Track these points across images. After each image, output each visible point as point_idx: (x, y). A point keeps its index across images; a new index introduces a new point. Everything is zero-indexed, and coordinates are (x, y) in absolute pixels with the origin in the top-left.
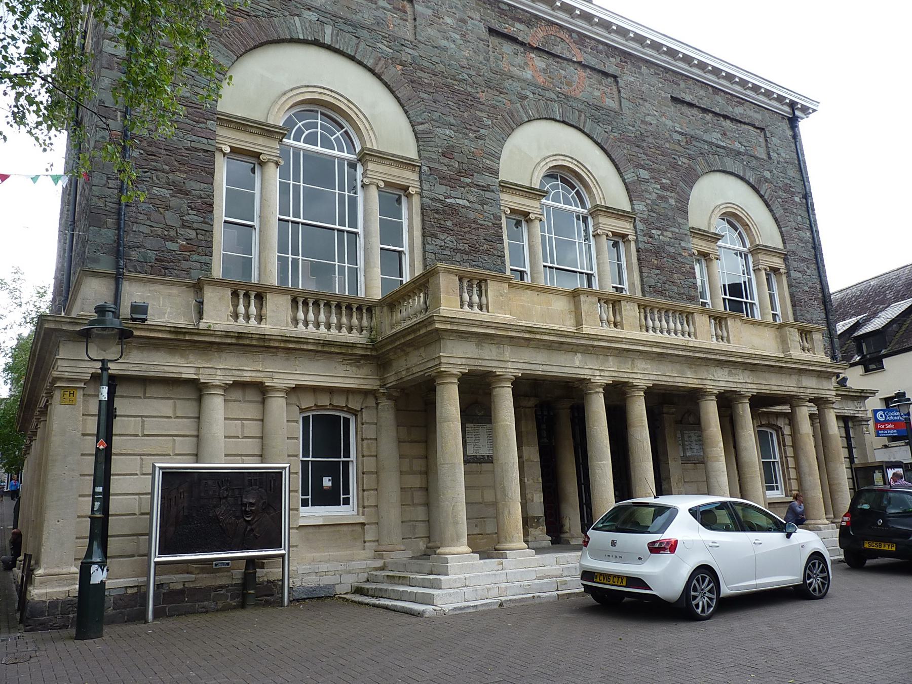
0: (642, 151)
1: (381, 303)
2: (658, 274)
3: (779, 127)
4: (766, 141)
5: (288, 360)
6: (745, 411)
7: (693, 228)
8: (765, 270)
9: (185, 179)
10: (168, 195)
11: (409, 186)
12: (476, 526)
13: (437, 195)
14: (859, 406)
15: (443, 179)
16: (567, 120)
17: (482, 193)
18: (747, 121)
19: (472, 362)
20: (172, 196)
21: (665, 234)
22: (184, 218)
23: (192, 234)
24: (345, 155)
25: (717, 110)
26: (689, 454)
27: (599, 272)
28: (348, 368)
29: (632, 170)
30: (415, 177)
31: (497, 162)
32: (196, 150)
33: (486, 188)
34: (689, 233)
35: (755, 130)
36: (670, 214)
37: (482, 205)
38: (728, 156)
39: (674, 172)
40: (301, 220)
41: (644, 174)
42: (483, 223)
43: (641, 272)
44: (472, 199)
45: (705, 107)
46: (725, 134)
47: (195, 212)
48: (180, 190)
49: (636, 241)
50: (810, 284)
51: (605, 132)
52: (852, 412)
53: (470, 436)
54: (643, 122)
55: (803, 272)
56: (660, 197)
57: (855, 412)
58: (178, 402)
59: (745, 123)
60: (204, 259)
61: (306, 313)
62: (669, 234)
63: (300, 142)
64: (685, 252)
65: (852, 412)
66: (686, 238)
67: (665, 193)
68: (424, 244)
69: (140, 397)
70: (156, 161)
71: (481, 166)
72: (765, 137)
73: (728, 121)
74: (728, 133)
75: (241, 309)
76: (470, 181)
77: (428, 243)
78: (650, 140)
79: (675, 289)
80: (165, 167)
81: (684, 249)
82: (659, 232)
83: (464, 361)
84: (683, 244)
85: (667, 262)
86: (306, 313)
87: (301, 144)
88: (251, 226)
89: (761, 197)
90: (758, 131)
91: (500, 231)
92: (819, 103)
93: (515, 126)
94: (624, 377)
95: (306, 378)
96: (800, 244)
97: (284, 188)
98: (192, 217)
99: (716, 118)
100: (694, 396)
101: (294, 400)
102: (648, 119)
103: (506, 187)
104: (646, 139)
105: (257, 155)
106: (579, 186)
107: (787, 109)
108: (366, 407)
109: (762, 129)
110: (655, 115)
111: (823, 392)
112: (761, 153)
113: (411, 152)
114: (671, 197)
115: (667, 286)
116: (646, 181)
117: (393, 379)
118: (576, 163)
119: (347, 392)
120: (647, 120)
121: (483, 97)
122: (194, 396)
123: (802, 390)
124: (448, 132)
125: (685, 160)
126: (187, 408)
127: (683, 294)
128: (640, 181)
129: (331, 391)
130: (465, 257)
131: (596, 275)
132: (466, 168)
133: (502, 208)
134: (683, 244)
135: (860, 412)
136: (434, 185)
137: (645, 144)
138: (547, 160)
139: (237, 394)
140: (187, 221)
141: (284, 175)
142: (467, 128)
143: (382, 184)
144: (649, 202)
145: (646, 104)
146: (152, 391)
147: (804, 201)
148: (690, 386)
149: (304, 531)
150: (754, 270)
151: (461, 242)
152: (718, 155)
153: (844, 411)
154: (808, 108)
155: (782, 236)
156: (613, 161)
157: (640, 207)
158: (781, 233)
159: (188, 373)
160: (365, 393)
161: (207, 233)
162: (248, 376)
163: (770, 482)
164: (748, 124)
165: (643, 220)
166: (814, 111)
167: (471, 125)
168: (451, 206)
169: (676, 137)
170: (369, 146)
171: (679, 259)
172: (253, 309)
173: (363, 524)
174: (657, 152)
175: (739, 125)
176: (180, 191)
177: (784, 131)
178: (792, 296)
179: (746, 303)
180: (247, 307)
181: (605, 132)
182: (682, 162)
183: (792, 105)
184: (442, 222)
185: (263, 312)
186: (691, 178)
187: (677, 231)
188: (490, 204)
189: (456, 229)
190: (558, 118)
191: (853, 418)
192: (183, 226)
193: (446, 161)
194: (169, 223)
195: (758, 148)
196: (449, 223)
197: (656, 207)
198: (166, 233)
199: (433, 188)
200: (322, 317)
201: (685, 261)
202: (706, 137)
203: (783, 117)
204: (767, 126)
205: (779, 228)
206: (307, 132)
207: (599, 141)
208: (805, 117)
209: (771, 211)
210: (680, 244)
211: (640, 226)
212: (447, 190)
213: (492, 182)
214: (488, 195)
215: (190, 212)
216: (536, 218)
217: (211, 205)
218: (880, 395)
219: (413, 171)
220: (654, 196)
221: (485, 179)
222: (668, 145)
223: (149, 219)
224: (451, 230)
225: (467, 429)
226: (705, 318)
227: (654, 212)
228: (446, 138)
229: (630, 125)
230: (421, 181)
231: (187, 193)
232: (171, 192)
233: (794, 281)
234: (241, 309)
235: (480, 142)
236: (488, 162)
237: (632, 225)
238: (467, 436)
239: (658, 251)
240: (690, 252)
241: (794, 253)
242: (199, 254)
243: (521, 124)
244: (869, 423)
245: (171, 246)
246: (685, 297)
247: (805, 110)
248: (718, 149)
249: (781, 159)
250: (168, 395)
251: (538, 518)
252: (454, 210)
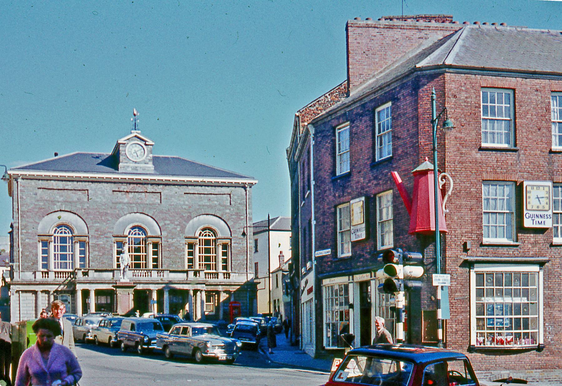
48: (31, 252)
102: (172, 204)
116: (168, 224)
121: (109, 212)
145: (173, 199)
168: (97, 244)
169: (184, 207)
172: (47, 275)
196: (96, 249)
235: (107, 225)
252: (98, 245)
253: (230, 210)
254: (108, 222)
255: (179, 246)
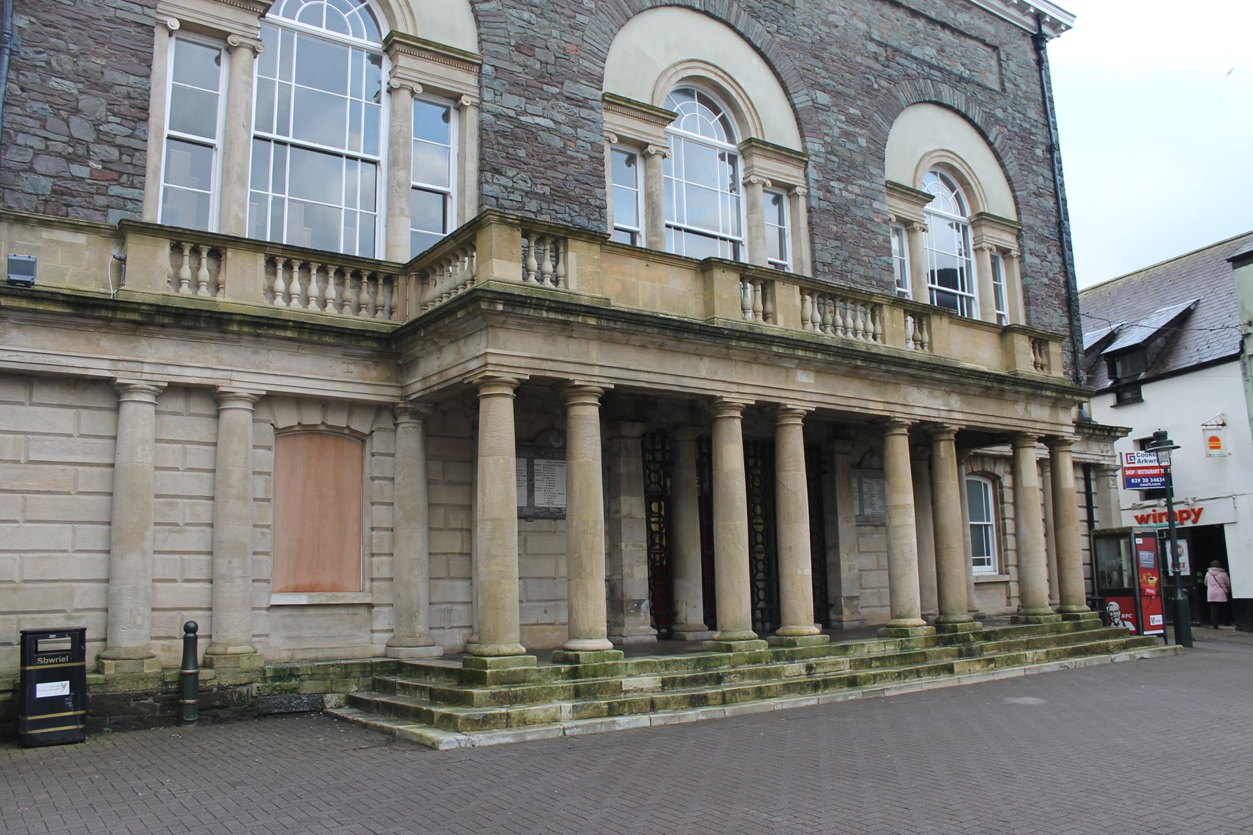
0: (820, 65)
1: (406, 269)
2: (837, 247)
3: (1019, 46)
4: (1000, 65)
5: (256, 352)
6: (946, 452)
7: (891, 183)
8: (991, 250)
9: (103, 66)
10: (75, 92)
11: (462, 95)
12: (546, 612)
13: (505, 110)
14: (1105, 449)
15: (516, 86)
16: (711, 11)
17: (576, 110)
18: (974, 33)
19: (536, 364)
20: (81, 92)
21: (850, 188)
22: (101, 128)
23: (114, 153)
24: (364, 42)
25: (933, 14)
26: (868, 512)
27: (749, 239)
28: (352, 368)
29: (806, 91)
30: (472, 79)
31: (602, 65)
32: (125, 22)
33: (583, 103)
34: (885, 190)
35: (985, 48)
36: (859, 159)
37: (575, 128)
38: (944, 82)
39: (867, 100)
40: (290, 139)
41: (823, 98)
42: (576, 154)
43: (812, 242)
44: (559, 117)
45: (916, 8)
46: (943, 51)
47: (118, 120)
48: (96, 85)
49: (808, 196)
50: (1051, 275)
51: (768, 32)
52: (1096, 457)
53: (540, 478)
54: (825, 22)
55: (1043, 258)
56: (846, 134)
57: (1100, 458)
58: (82, 412)
59: (971, 37)
60: (129, 193)
61: (288, 282)
62: (857, 190)
63: (294, 19)
64: (878, 217)
65: (1096, 457)
66: (881, 197)
67: (851, 129)
68: (480, 183)
69: (22, 404)
70: (59, 37)
71: (575, 69)
72: (999, 59)
73: (947, 32)
74: (947, 49)
75: (186, 272)
76: (557, 90)
77: (487, 182)
78: (834, 49)
79: (861, 270)
80: (72, 46)
81: (877, 212)
82: (842, 186)
83: (524, 363)
84: (876, 205)
85: (851, 229)
86: (288, 282)
87: (295, 23)
88: (211, 146)
89: (990, 144)
90: (990, 50)
91: (601, 168)
92: (1074, 17)
93: (631, 13)
94: (772, 396)
95: (285, 381)
96: (1040, 217)
97: (265, 86)
98: (113, 127)
99: (931, 26)
100: (879, 427)
101: (265, 414)
102: (832, 18)
103: (614, 102)
104: (828, 47)
105: (223, 36)
106: (725, 110)
107: (1030, 21)
108: (379, 429)
109: (995, 48)
110: (843, 14)
111: (1058, 428)
112: (992, 81)
113: (467, 41)
114: (861, 135)
115: (849, 265)
116: (825, 108)
117: (418, 386)
118: (721, 74)
119: (351, 406)
120: (830, 19)
122: (109, 404)
123: (1029, 424)
124: (526, 15)
125: (884, 83)
126: (99, 421)
127: (873, 278)
128: (817, 107)
129: (324, 403)
130: (545, 205)
131: (745, 242)
132: (553, 72)
133: (605, 134)
134: (876, 205)
135: (1107, 458)
136: (501, 95)
137: (825, 55)
138: (678, 68)
139: (176, 404)
140: (106, 133)
141: (266, 69)
142: (556, 12)
143: (419, 89)
144: (828, 139)
146: (42, 394)
147: (1048, 156)
148: (871, 412)
149: (279, 613)
150: (975, 250)
151: (539, 181)
152: (932, 80)
153: (1084, 456)
154: (1060, 23)
155: (1017, 203)
156: (777, 75)
157: (815, 146)
158: (1015, 198)
159: (99, 368)
160: (376, 408)
161: (137, 154)
162: (192, 376)
163: (979, 553)
164: (976, 39)
165: (818, 166)
166: (1068, 28)
167: (563, 8)
170: (401, 29)
171: (869, 226)
172: (204, 274)
173: (370, 606)
174: (843, 67)
175: (963, 39)
176: (96, 85)
177: (1025, 53)
178: (1026, 289)
179: (961, 296)
180: (196, 269)
181: (768, 32)
182: (879, 85)
183: (1039, 16)
184: (511, 151)
185: (221, 278)
186: (892, 111)
187: (867, 185)
188: (587, 128)
189: (531, 161)
190: (697, 6)
191: (1097, 467)
192: (98, 141)
193: (521, 59)
194: (77, 135)
195: (988, 74)
197: (837, 148)
198: (70, 150)
199: (498, 98)
200: (314, 289)
201: (878, 230)
202: (916, 52)
203: (1025, 33)
204: (1002, 44)
205: (1013, 191)
206: (305, 5)
207: (758, 45)
208: (1055, 35)
209: (1002, 166)
210: (871, 205)
211: (813, 174)
212: (520, 102)
213: (592, 94)
214: (584, 113)
215: (111, 118)
216: (657, 153)
217: (145, 109)
218: (1133, 436)
219: (469, 71)
220: (836, 132)
221: (584, 90)
222: (859, 59)
223: (43, 127)
224: (525, 164)
225: (536, 467)
226: (899, 313)
227: (836, 155)
228: (523, 24)
229: (804, 25)
230: (480, 87)
231: (106, 88)
232: (81, 86)
233: (1028, 269)
234: (186, 272)
235: (578, 33)
236: (587, 64)
237: (802, 172)
238: (536, 478)
239: (840, 212)
240: (885, 217)
241: (1030, 228)
242: (122, 185)
243: (641, 11)
244: (1117, 473)
245: (78, 170)
246: (874, 283)
247: (1057, 26)
248: (932, 71)
249: (1020, 93)
250: (68, 402)
251: (640, 602)
252: (531, 133)
253: (1005, 110)
254: (580, 18)
255: (871, 220)
